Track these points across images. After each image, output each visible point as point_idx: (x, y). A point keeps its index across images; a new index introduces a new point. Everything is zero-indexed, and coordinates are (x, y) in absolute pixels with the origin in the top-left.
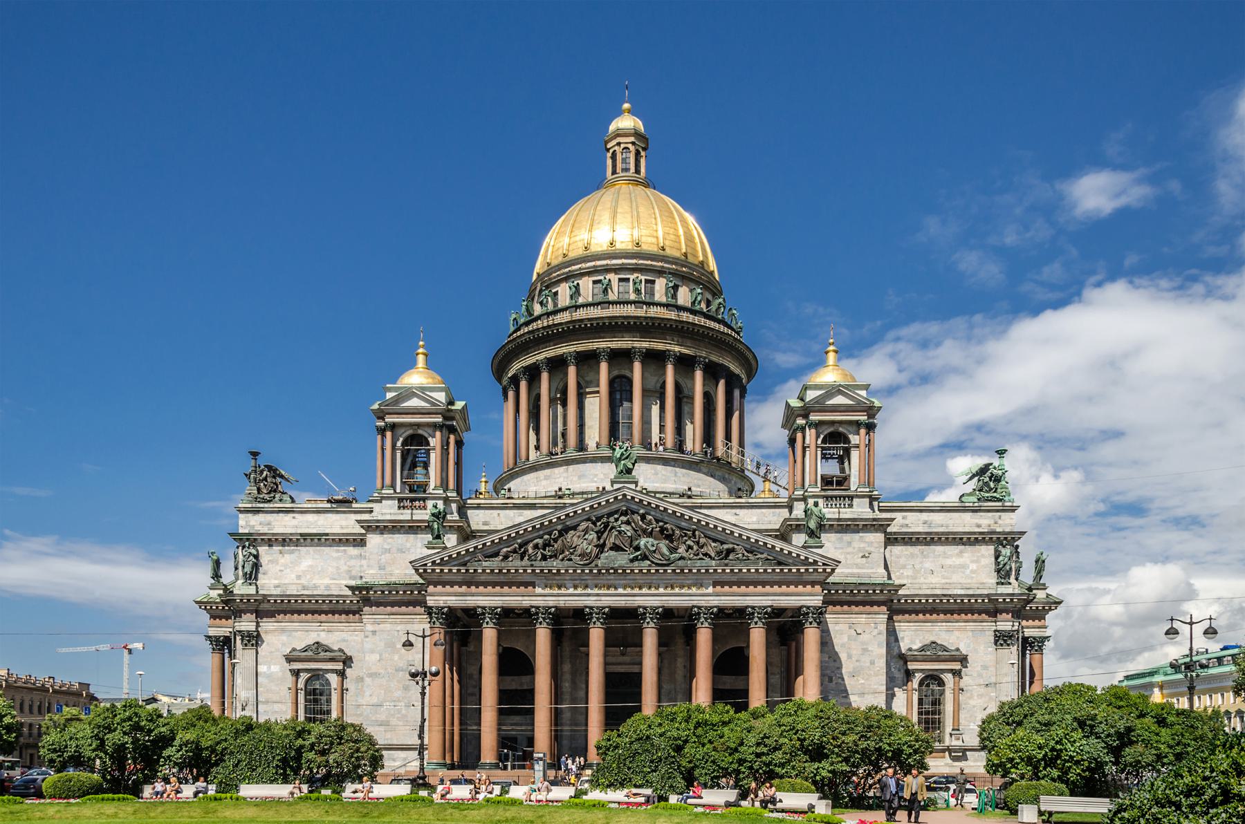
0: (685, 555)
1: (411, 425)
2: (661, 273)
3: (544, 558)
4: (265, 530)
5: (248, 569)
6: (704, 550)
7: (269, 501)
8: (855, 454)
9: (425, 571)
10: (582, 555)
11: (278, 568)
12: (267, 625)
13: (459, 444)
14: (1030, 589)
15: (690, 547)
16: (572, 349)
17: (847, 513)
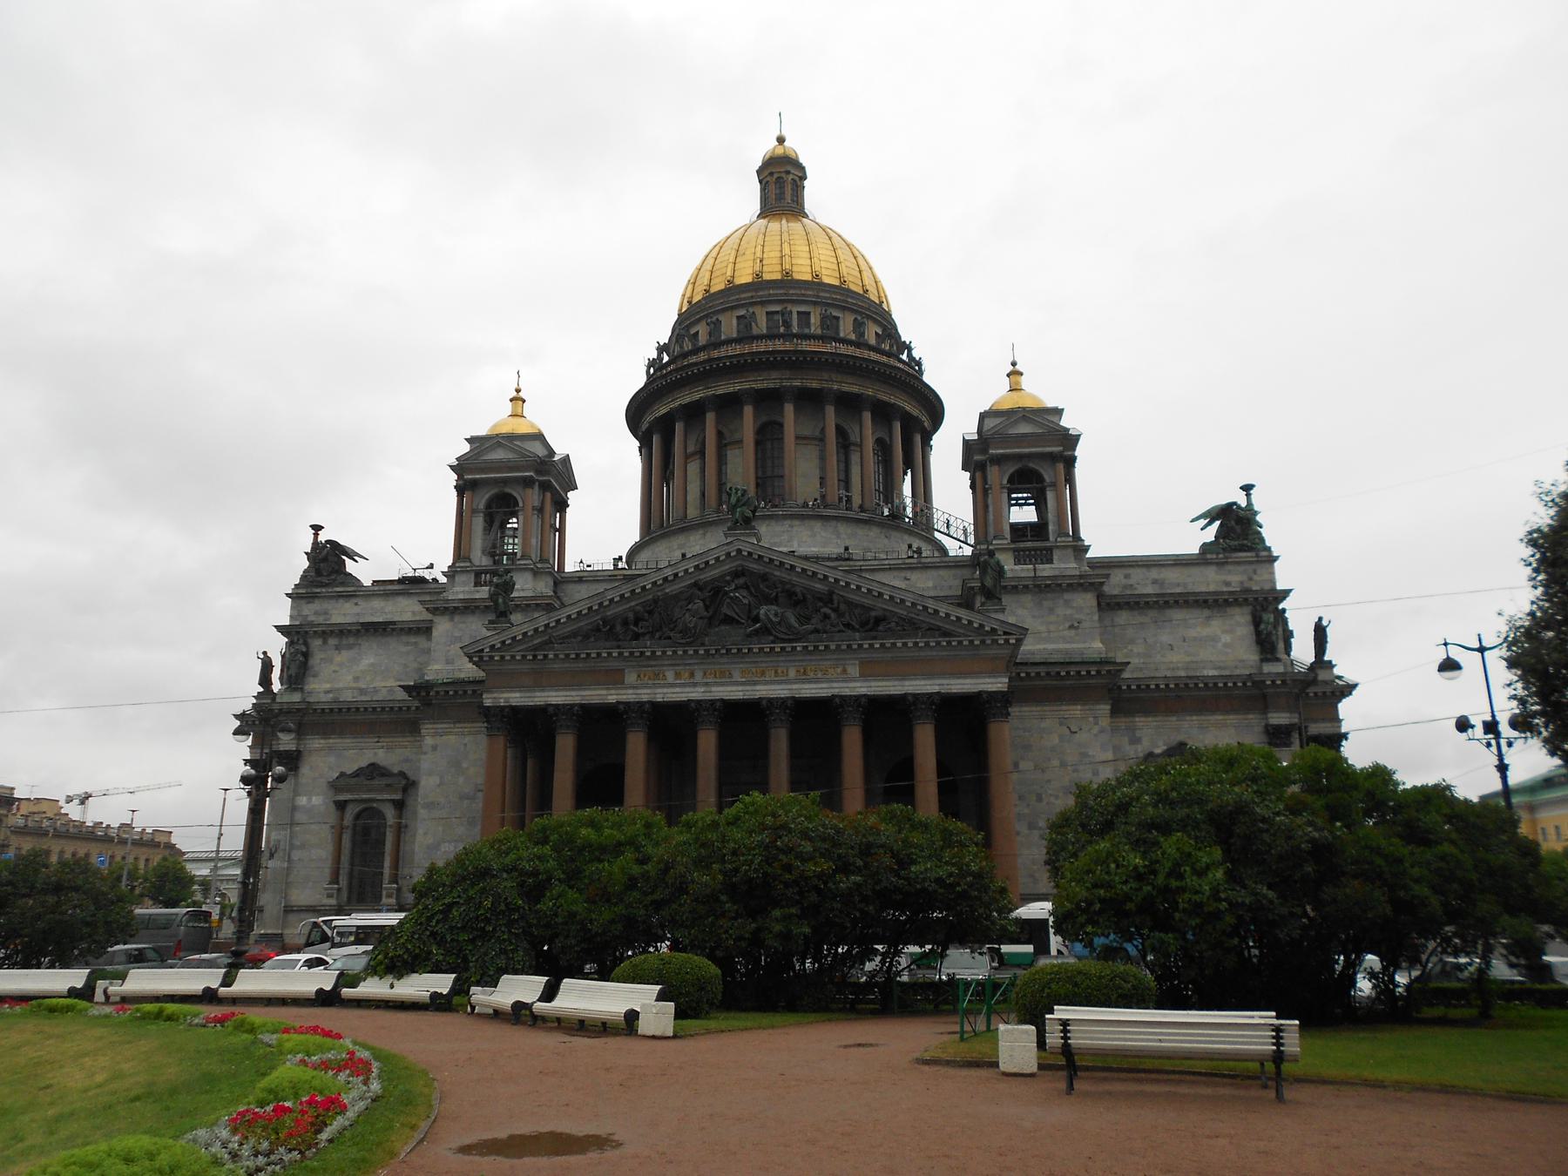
0: (820, 627)
1: (496, 481)
2: (815, 303)
3: (636, 637)
4: (321, 620)
5: (293, 672)
6: (847, 619)
7: (326, 585)
8: (1050, 495)
9: (481, 658)
10: (685, 631)
11: (333, 668)
12: (315, 743)
13: (562, 506)
14: (1312, 667)
15: (826, 617)
16: (711, 392)
17: (1045, 570)
